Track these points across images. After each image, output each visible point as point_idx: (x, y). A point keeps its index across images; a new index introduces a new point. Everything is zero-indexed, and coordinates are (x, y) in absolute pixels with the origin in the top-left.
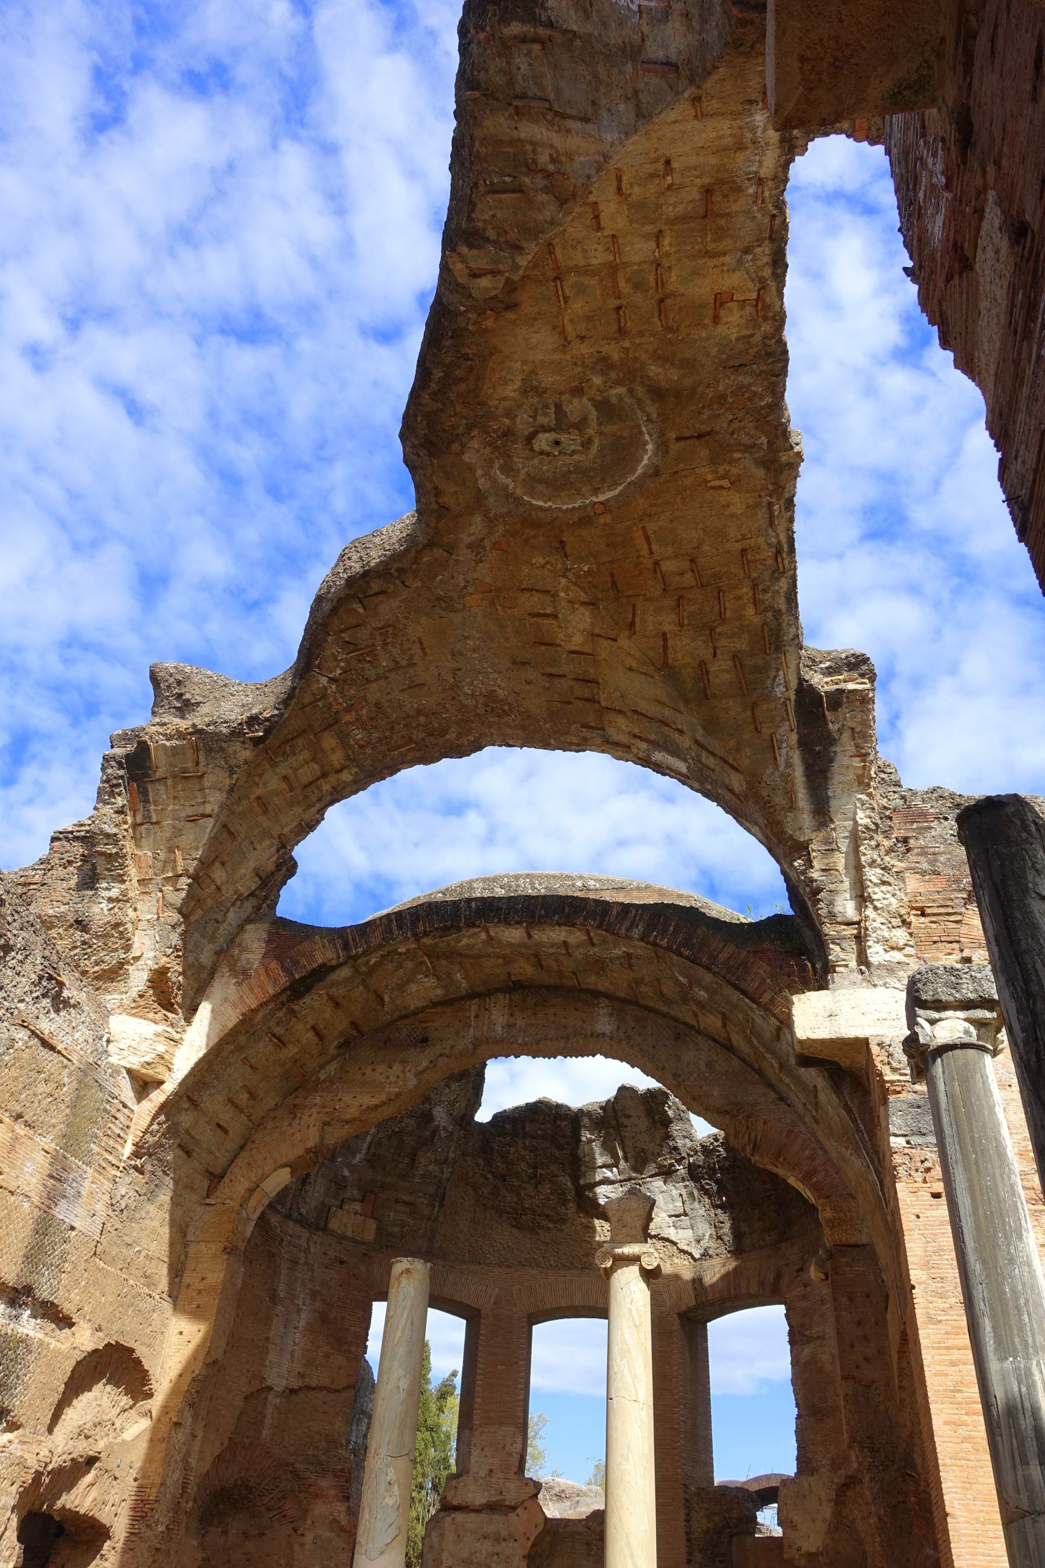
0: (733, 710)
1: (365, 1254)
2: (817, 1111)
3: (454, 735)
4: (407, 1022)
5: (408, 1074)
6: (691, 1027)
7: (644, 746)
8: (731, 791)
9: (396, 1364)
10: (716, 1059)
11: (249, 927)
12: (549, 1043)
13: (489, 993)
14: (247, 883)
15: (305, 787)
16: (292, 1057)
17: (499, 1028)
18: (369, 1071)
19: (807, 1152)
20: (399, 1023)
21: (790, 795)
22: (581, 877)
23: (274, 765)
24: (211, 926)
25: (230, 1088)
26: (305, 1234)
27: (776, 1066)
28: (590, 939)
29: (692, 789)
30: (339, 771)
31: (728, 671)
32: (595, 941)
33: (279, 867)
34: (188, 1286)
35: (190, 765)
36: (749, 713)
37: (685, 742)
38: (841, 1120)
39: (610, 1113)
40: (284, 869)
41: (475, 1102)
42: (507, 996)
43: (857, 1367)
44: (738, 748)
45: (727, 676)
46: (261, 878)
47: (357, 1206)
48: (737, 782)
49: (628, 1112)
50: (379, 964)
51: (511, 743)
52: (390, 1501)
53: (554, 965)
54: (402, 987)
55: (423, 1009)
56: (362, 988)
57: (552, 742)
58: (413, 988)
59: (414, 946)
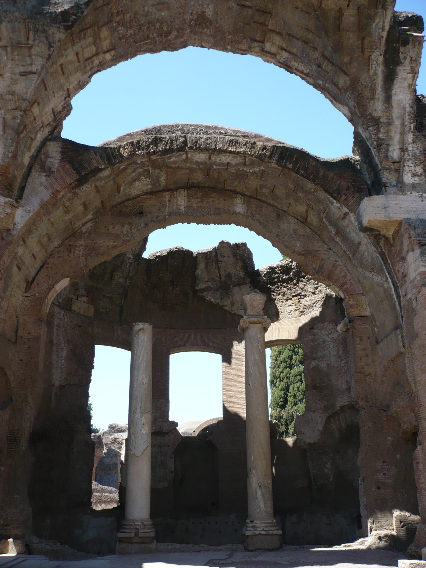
0: (351, 38)
2: (353, 255)
3: (173, 37)
4: (130, 202)
5: (133, 231)
6: (284, 211)
7: (285, 55)
8: (336, 85)
9: (141, 372)
10: (298, 228)
11: (48, 143)
13: (176, 189)
14: (48, 118)
15: (86, 60)
16: (71, 219)
17: (182, 208)
19: (342, 274)
20: (126, 203)
21: (373, 91)
22: (222, 128)
23: (73, 45)
24: (29, 141)
25: (40, 234)
26: (62, 312)
27: (333, 232)
28: (245, 162)
29: (308, 82)
30: (105, 53)
31: (353, 16)
32: (247, 163)
33: (64, 108)
34: (22, 337)
35: (23, 39)
36: (360, 42)
37: (316, 55)
38: (373, 258)
39: (214, 254)
40: (66, 110)
41: (143, 248)
42: (186, 191)
43: (363, 368)
44: (350, 62)
45: (353, 19)
46: (54, 115)
47: (85, 299)
48: (343, 81)
50: (125, 169)
51: (204, 45)
52: (144, 432)
53: (216, 175)
54: (132, 183)
55: (138, 196)
56: (112, 182)
57: (229, 47)
58: (137, 183)
59: (146, 160)
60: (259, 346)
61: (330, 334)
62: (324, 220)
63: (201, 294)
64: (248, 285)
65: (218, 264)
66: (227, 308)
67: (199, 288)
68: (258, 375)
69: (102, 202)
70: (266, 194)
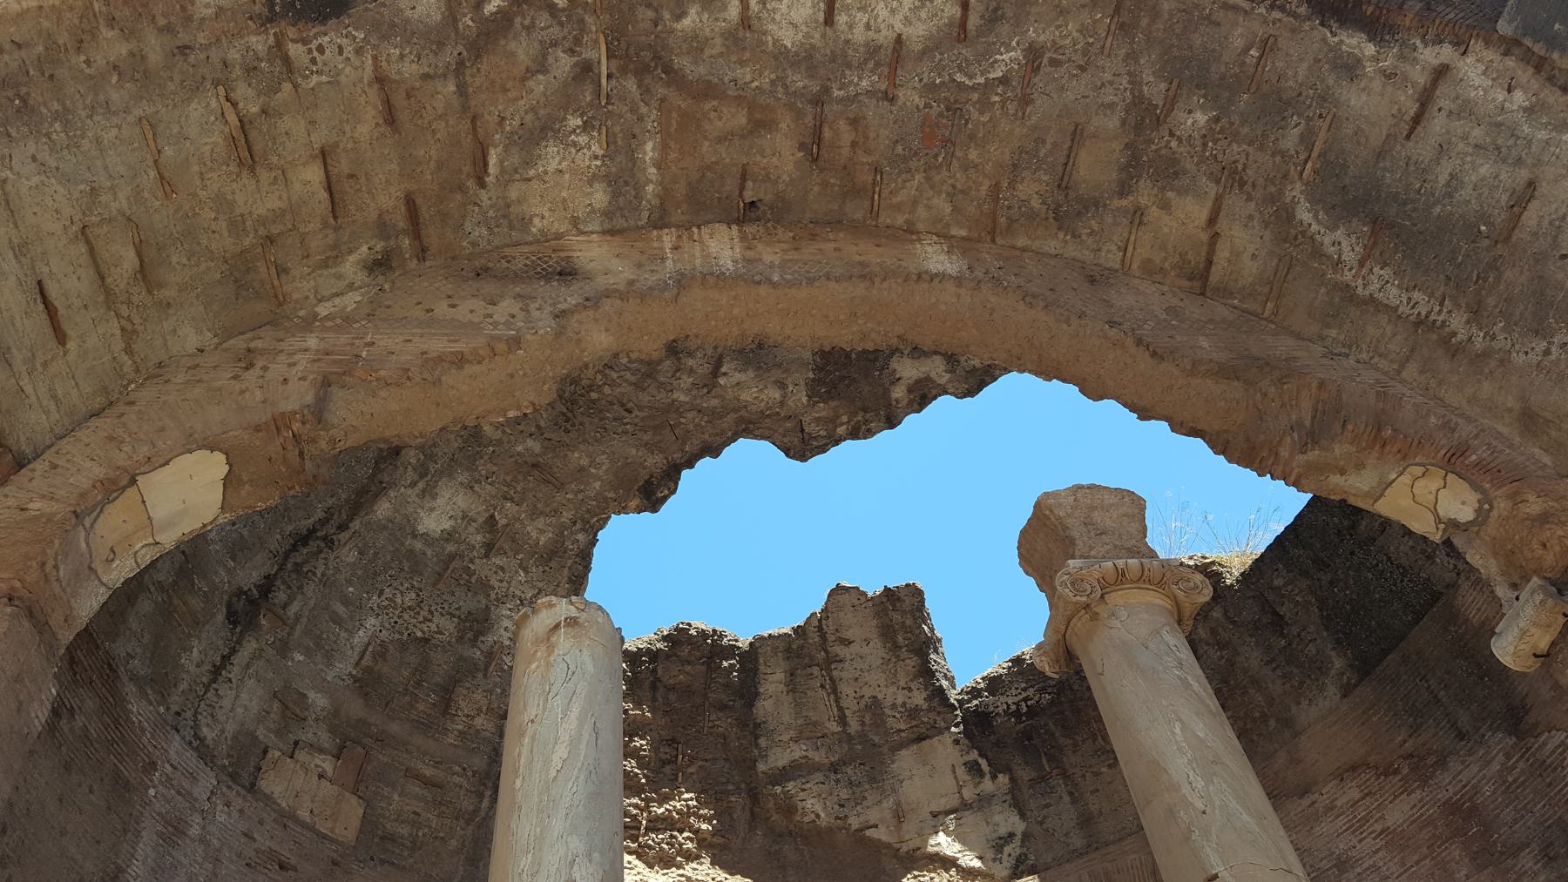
1: (335, 863)
5: (536, 314)
12: (832, 284)
16: (262, 221)
18: (442, 309)
32: (973, 21)
39: (814, 638)
42: (735, 227)
49: (848, 635)
60: (1195, 685)
61: (1365, 819)
62: (1304, 214)
63: (778, 789)
65: (829, 670)
66: (881, 834)
68: (1245, 817)
69: (410, 203)
70: (1035, 203)
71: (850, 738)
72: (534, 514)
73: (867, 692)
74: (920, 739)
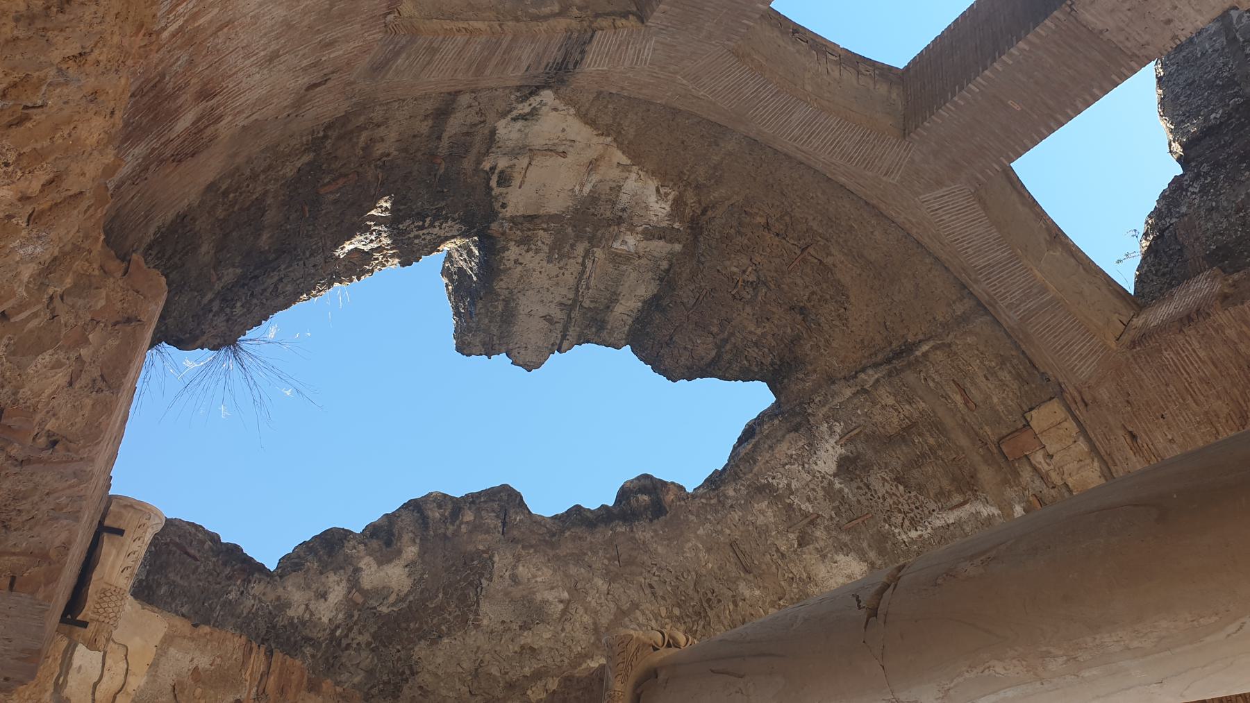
39: (573, 332)
47: (1038, 458)
63: (676, 225)
64: (509, 212)
65: (575, 301)
66: (620, 157)
67: (669, 246)
71: (591, 240)
72: (764, 531)
73: (553, 269)
74: (531, 218)
